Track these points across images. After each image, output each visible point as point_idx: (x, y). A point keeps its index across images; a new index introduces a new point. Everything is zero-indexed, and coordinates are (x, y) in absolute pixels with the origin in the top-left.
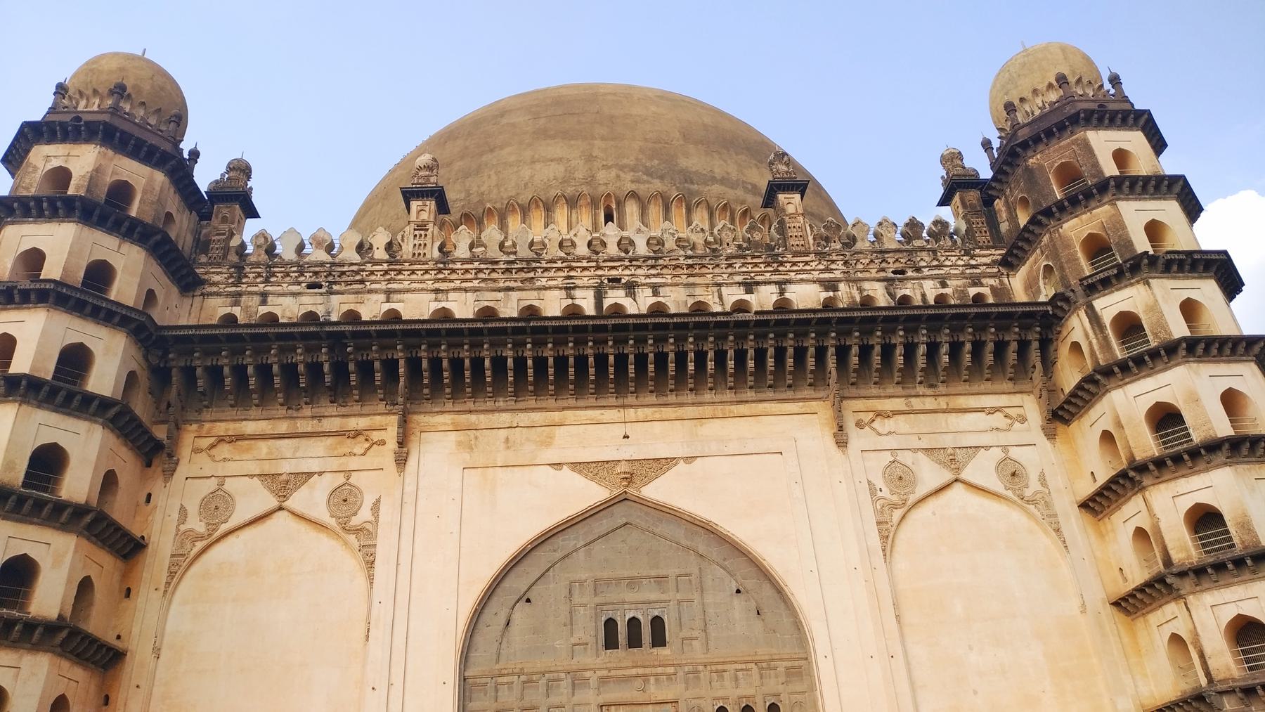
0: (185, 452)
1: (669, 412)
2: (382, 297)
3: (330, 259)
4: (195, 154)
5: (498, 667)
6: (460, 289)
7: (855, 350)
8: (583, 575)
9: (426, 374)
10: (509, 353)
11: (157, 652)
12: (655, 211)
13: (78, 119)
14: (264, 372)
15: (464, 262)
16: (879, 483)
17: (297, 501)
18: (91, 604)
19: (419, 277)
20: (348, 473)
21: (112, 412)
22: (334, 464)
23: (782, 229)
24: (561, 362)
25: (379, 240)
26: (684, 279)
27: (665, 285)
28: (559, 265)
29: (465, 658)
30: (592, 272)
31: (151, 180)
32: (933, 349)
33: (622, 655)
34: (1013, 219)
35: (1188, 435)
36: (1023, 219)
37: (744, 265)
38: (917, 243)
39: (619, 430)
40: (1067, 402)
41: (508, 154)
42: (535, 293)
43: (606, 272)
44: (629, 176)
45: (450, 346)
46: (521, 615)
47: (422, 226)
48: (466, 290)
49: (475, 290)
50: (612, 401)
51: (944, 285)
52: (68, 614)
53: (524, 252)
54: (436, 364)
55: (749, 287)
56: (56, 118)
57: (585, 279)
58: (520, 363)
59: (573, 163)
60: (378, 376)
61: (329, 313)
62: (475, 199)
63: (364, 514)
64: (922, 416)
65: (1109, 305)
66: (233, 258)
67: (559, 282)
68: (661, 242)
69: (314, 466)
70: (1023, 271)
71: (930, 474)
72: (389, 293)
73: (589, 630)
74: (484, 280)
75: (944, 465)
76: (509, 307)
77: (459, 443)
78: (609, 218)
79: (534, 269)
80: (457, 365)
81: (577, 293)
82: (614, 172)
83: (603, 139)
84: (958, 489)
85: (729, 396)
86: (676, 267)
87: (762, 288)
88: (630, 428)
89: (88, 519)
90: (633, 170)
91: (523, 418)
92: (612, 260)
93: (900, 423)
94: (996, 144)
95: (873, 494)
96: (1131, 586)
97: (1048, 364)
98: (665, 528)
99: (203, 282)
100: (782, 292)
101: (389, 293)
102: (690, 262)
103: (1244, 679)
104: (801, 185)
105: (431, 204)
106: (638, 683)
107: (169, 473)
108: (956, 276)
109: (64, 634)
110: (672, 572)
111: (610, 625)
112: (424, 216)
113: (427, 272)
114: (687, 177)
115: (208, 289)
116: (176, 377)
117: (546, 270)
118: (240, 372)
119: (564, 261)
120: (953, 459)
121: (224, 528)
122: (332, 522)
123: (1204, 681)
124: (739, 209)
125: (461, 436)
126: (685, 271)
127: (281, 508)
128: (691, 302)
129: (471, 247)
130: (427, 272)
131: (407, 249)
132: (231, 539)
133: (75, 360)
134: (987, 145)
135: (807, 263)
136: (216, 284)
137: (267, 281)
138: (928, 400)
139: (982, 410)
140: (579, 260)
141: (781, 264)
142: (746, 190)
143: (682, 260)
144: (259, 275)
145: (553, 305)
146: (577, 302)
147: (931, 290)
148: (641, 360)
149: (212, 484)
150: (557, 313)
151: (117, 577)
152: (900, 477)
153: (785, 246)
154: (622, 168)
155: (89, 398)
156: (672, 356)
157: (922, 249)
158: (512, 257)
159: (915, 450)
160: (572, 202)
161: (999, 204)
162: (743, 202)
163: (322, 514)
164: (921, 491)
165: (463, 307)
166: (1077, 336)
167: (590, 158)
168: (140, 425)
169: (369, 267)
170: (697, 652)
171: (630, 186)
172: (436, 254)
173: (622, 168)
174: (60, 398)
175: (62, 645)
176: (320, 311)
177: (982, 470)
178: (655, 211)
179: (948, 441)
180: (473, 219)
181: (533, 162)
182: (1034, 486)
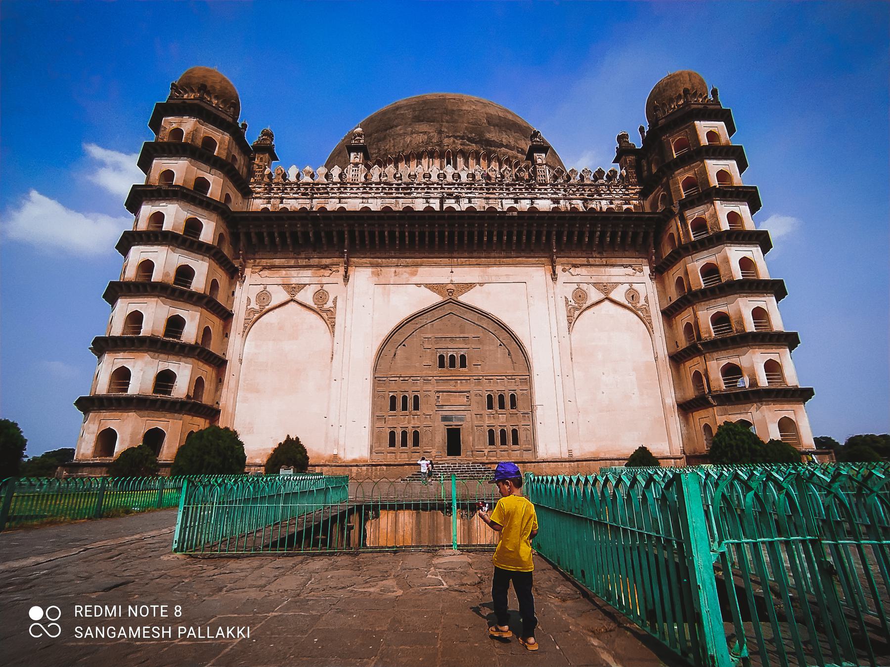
0: (248, 271)
2: (337, 201)
3: (310, 180)
4: (245, 126)
6: (374, 198)
7: (566, 233)
9: (357, 239)
10: (397, 229)
11: (241, 361)
12: (471, 162)
13: (185, 102)
14: (282, 235)
15: (376, 184)
16: (570, 299)
17: (299, 297)
18: (210, 339)
19: (355, 190)
20: (322, 284)
21: (213, 252)
22: (315, 280)
23: (535, 171)
24: (422, 235)
25: (336, 171)
26: (485, 195)
27: (475, 198)
28: (423, 186)
29: (375, 369)
30: (439, 190)
31: (222, 139)
34: (649, 169)
35: (720, 279)
36: (654, 170)
37: (515, 189)
38: (600, 181)
39: (449, 269)
40: (664, 263)
41: (399, 130)
43: (446, 190)
44: (459, 142)
45: (369, 225)
47: (356, 165)
48: (376, 198)
49: (381, 198)
50: (446, 255)
52: (200, 342)
53: (406, 179)
54: (362, 233)
55: (516, 201)
56: (172, 101)
57: (436, 194)
58: (402, 234)
59: (432, 134)
60: (335, 239)
61: (312, 208)
62: (382, 152)
63: (330, 304)
65: (692, 214)
66: (266, 180)
67: (423, 195)
68: (473, 176)
69: (307, 280)
70: (651, 197)
71: (594, 295)
72: (340, 198)
73: (431, 360)
74: (385, 193)
75: (602, 291)
76: (399, 205)
77: (373, 273)
78: (449, 163)
79: (411, 189)
80: (372, 234)
81: (431, 201)
82: (452, 139)
83: (447, 122)
84: (607, 302)
85: (503, 254)
86: (481, 189)
88: (454, 269)
89: (205, 300)
90: (462, 138)
91: (403, 261)
92: (449, 184)
93: (583, 271)
94: (647, 129)
95: (567, 303)
96: (680, 349)
97: (658, 245)
98: (470, 315)
100: (532, 203)
101: (340, 198)
103: (725, 391)
104: (544, 148)
105: (361, 155)
108: (617, 199)
109: (198, 350)
110: (471, 335)
111: (441, 357)
112: (357, 160)
113: (358, 188)
114: (489, 143)
115: (254, 195)
116: (242, 237)
117: (416, 189)
118: (271, 235)
119: (425, 184)
120: (605, 288)
121: (267, 307)
122: (316, 307)
123: (707, 391)
124: (514, 161)
125: (374, 270)
127: (292, 300)
128: (487, 207)
129: (380, 176)
130: (358, 188)
131: (349, 176)
132: (271, 312)
133: (193, 226)
134: (642, 129)
135: (545, 189)
136: (259, 193)
137: (283, 192)
139: (622, 265)
140: (433, 184)
141: (533, 189)
142: (518, 152)
144: (279, 189)
145: (419, 205)
147: (605, 205)
148: (461, 235)
149: (261, 288)
150: (421, 209)
151: (221, 328)
152: (580, 295)
153: (535, 180)
155: (202, 244)
156: (476, 233)
157: (603, 184)
158: (400, 182)
160: (431, 155)
161: (644, 162)
162: (516, 158)
163: (310, 302)
164: (589, 303)
165: (375, 205)
166: (673, 230)
167: (440, 132)
168: (227, 259)
169: (331, 186)
170: (479, 371)
171: (459, 147)
172: (363, 179)
173: (456, 137)
174: (188, 243)
175: (198, 355)
176: (308, 207)
177: (619, 294)
178: (471, 162)
179: (604, 279)
180: (382, 164)
181: (412, 133)
182: (642, 301)
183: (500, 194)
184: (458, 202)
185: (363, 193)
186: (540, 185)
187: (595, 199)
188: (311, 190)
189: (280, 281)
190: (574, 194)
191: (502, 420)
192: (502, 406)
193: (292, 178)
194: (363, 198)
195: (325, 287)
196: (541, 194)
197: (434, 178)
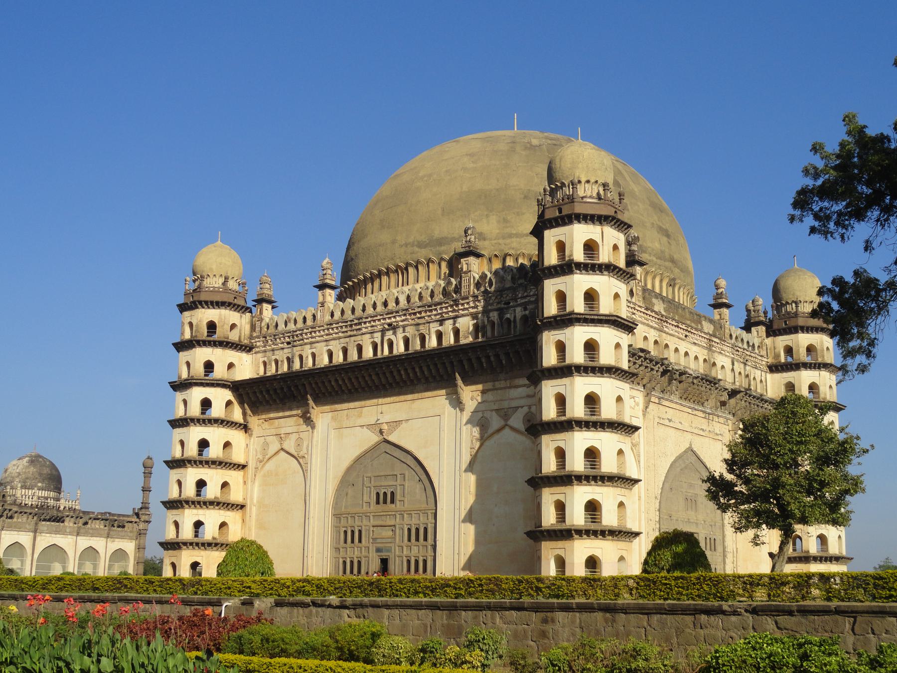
1: (402, 398)
2: (309, 346)
5: (343, 510)
8: (369, 475)
19: (322, 333)
26: (418, 321)
27: (408, 325)
28: (369, 319)
31: (220, 315)
32: (497, 356)
33: (382, 506)
37: (441, 308)
42: (359, 338)
43: (388, 321)
46: (350, 491)
49: (340, 338)
51: (525, 309)
55: (441, 322)
63: (305, 451)
64: (499, 391)
69: (289, 430)
77: (332, 417)
79: (360, 324)
81: (376, 335)
84: (507, 431)
86: (415, 314)
87: (447, 322)
88: (385, 408)
90: (413, 246)
98: (398, 453)
99: (256, 347)
100: (454, 324)
101: (311, 343)
102: (420, 309)
106: (383, 518)
107: (251, 435)
111: (378, 494)
114: (441, 242)
116: (245, 398)
117: (365, 323)
121: (267, 457)
126: (418, 315)
138: (502, 382)
141: (457, 305)
143: (417, 310)
146: (376, 340)
154: (406, 245)
159: (492, 410)
163: (293, 452)
164: (490, 431)
167: (394, 242)
169: (305, 331)
177: (517, 421)
179: (506, 404)
183: (429, 316)
184: (395, 333)
185: (327, 335)
186: (463, 299)
187: (512, 307)
188: (293, 339)
189: (274, 432)
190: (492, 304)
191: (416, 551)
192: (417, 539)
193: (281, 327)
194: (326, 341)
195: (302, 435)
196: (463, 310)
197: (380, 308)
